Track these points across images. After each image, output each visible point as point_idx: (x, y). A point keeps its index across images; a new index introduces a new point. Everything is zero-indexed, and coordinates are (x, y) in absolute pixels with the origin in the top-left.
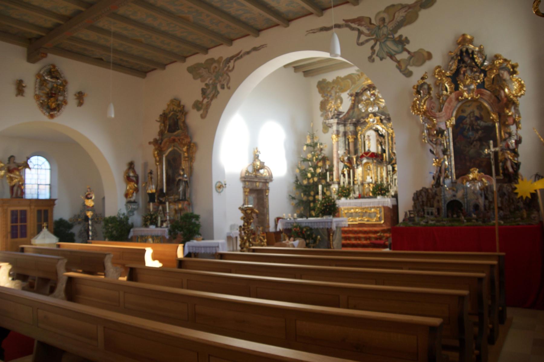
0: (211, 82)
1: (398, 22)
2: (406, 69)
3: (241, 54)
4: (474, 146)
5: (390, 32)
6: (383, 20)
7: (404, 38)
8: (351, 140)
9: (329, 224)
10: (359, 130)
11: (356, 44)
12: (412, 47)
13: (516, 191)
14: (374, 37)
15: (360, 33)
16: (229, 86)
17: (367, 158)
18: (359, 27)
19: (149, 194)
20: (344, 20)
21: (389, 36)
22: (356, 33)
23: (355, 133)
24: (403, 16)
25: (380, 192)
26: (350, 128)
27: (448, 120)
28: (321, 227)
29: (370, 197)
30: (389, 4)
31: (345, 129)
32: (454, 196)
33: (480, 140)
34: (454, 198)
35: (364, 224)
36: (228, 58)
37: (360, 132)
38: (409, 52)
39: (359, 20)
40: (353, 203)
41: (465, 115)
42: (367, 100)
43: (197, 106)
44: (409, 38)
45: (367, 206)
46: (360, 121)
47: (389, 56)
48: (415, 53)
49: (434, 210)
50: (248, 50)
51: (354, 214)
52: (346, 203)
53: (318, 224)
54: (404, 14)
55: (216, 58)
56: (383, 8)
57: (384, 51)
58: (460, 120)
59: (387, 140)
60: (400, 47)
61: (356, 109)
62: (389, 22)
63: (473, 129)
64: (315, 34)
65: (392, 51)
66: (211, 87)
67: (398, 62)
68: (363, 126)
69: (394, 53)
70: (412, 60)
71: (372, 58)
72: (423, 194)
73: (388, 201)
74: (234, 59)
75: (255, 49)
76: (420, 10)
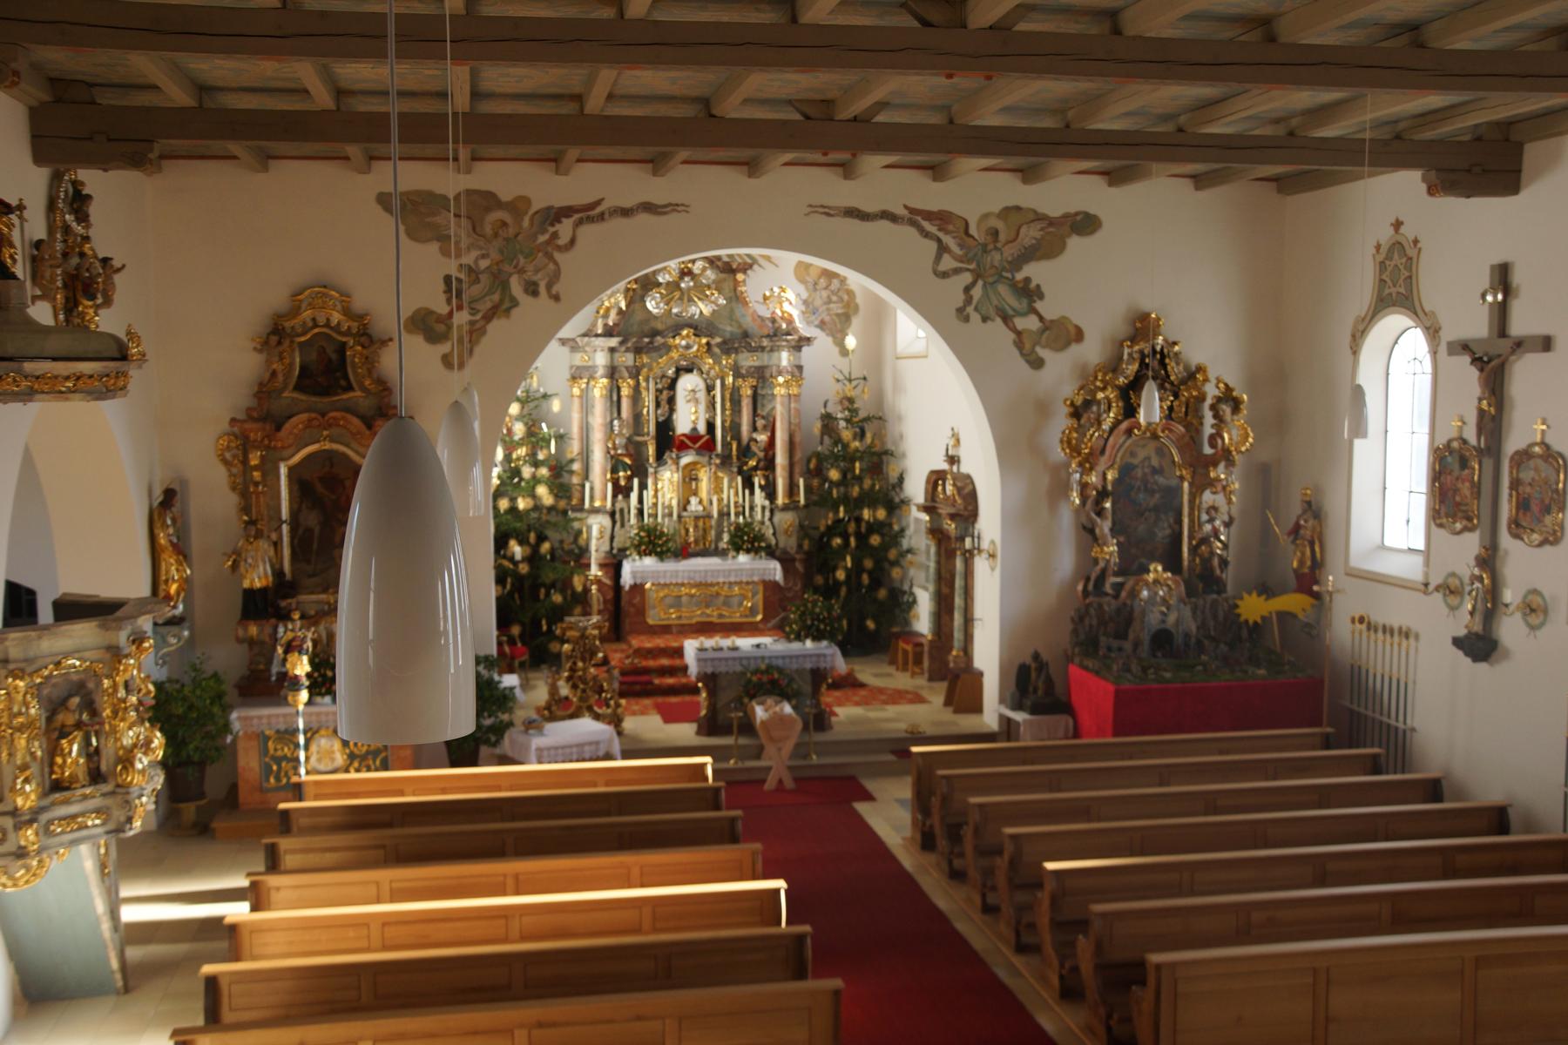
0: (484, 264)
1: (1025, 248)
2: (1033, 351)
3: (598, 210)
4: (1146, 519)
5: (1005, 264)
6: (995, 233)
7: (1033, 285)
10: (643, 366)
11: (931, 270)
12: (1049, 308)
13: (1238, 611)
14: (972, 266)
15: (942, 249)
16: (554, 291)
17: (699, 451)
18: (941, 235)
19: (250, 594)
20: (906, 207)
21: (1005, 274)
22: (933, 246)
23: (635, 373)
24: (1035, 239)
26: (627, 359)
27: (1108, 468)
28: (808, 666)
29: (722, 553)
30: (1010, 203)
31: (612, 359)
32: (1163, 622)
33: (1156, 509)
34: (1163, 626)
35: (711, 623)
36: (549, 208)
38: (1041, 318)
39: (942, 218)
40: (684, 571)
41: (1135, 461)
42: (668, 283)
43: (428, 325)
44: (1044, 289)
45: (721, 580)
47: (1000, 316)
48: (1052, 321)
49: (1128, 646)
50: (627, 204)
51: (684, 599)
52: (665, 572)
54: (1038, 234)
55: (505, 196)
56: (997, 211)
57: (991, 304)
58: (1126, 471)
60: (1025, 302)
61: (637, 306)
62: (1008, 242)
63: (1146, 490)
64: (831, 219)
65: (1007, 307)
66: (484, 278)
67: (1019, 333)
68: (654, 355)
69: (1011, 312)
70: (1048, 332)
71: (965, 313)
72: (1092, 611)
73: (775, 569)
74: (577, 216)
75: (649, 208)
76: (1069, 236)
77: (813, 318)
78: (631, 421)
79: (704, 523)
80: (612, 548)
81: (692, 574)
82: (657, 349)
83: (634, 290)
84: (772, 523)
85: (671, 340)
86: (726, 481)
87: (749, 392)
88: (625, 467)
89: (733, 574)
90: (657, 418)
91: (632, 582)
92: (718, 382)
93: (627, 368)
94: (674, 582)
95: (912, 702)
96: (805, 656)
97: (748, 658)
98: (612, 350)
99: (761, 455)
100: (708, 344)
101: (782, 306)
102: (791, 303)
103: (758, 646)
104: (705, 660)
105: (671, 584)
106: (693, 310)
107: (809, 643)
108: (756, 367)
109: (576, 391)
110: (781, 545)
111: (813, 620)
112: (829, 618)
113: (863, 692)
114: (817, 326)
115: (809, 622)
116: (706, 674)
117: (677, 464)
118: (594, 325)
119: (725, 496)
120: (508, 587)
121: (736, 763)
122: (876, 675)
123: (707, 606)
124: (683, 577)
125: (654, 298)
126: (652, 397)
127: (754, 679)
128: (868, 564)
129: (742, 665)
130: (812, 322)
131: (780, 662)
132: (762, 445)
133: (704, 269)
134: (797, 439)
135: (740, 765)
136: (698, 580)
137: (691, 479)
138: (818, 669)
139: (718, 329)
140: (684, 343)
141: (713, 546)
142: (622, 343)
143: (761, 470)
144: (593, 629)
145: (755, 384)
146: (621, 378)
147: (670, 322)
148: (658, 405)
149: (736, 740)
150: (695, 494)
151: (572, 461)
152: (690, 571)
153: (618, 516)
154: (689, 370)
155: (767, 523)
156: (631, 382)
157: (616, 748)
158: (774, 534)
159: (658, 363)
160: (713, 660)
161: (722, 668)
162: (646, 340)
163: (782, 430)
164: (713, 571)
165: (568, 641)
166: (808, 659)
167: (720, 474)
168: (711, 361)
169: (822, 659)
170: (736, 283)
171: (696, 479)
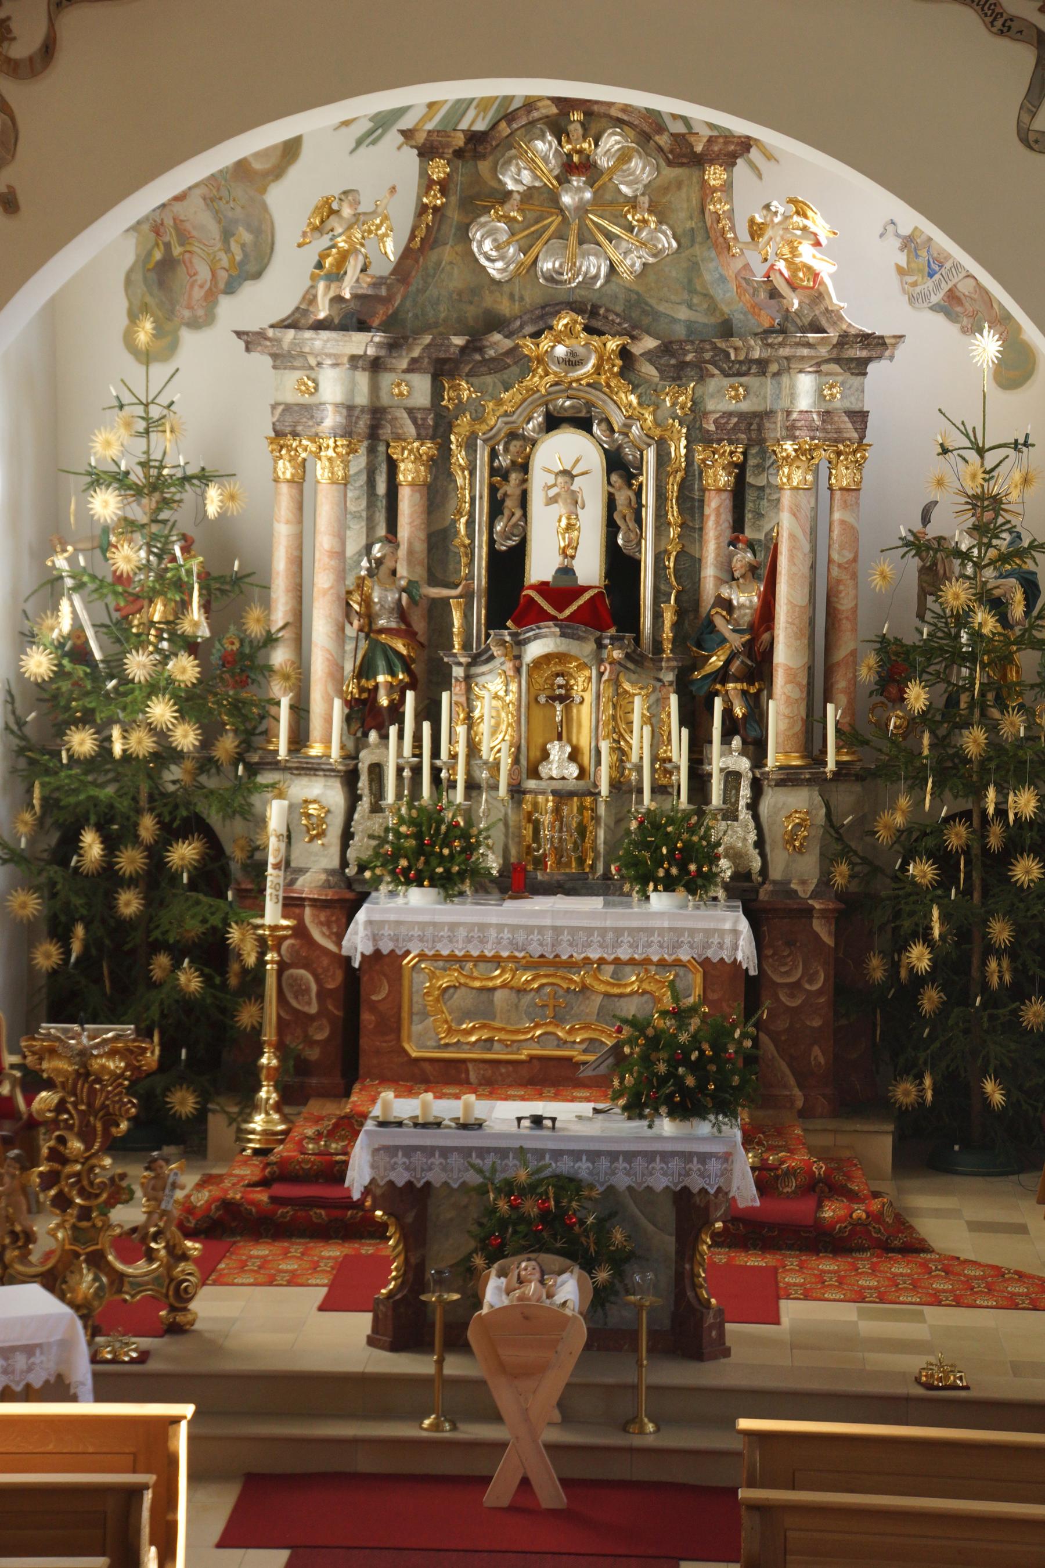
8: (408, 472)
9: (714, 1165)
10: (461, 408)
25: (674, 871)
28: (660, 1182)
31: (375, 388)
37: (464, 421)
40: (500, 927)
42: (529, 194)
45: (595, 955)
46: (480, 350)
52: (453, 926)
53: (640, 1163)
59: (649, 497)
61: (447, 253)
68: (489, 379)
73: (736, 932)
77: (930, 283)
78: (420, 547)
79: (581, 809)
80: (344, 863)
81: (521, 937)
82: (496, 365)
83: (436, 209)
84: (756, 817)
85: (529, 342)
86: (638, 707)
87: (724, 479)
88: (393, 661)
89: (626, 938)
90: (491, 542)
91: (369, 951)
92: (650, 455)
93: (410, 411)
94: (475, 953)
95: (1012, 1304)
96: (650, 1156)
97: (503, 1153)
98: (376, 366)
99: (737, 641)
100: (624, 353)
101: (794, 250)
102: (817, 244)
103: (537, 1121)
104: (391, 1150)
105: (467, 957)
106: (594, 265)
107: (667, 1126)
108: (742, 415)
109: (285, 469)
110: (776, 873)
111: (673, 1063)
112: (715, 1059)
113: (900, 1268)
114: (935, 308)
115: (662, 1068)
116: (391, 1183)
117: (518, 657)
118: (310, 299)
119: (634, 742)
120: (76, 947)
121: (436, 1427)
122: (975, 1227)
123: (558, 1020)
124: (499, 942)
125: (491, 233)
126: (482, 488)
127: (503, 1206)
128: (1001, 932)
129: (480, 1171)
130: (925, 297)
131: (583, 1169)
132: (745, 617)
133: (624, 157)
134: (845, 604)
135: (447, 1433)
136: (536, 950)
137: (554, 698)
138: (685, 1190)
139: (656, 315)
140: (561, 350)
141: (600, 869)
142: (393, 346)
143: (737, 680)
144: (112, 1054)
145: (738, 458)
146: (399, 438)
147: (532, 297)
148: (496, 509)
149: (440, 1363)
150: (560, 738)
151: (270, 640)
152: (514, 928)
153: (363, 783)
154: (584, 424)
155: (744, 815)
156: (427, 448)
157: (82, 1371)
158: (760, 844)
159: (500, 402)
160: (409, 1150)
161: (436, 1177)
162: (458, 341)
163: (792, 577)
164: (573, 930)
165: (49, 1085)
166: (658, 1164)
167: (627, 686)
168: (633, 399)
169: (695, 1165)
170: (706, 191)
171: (566, 699)
